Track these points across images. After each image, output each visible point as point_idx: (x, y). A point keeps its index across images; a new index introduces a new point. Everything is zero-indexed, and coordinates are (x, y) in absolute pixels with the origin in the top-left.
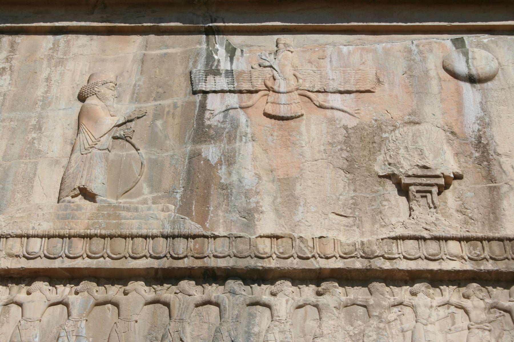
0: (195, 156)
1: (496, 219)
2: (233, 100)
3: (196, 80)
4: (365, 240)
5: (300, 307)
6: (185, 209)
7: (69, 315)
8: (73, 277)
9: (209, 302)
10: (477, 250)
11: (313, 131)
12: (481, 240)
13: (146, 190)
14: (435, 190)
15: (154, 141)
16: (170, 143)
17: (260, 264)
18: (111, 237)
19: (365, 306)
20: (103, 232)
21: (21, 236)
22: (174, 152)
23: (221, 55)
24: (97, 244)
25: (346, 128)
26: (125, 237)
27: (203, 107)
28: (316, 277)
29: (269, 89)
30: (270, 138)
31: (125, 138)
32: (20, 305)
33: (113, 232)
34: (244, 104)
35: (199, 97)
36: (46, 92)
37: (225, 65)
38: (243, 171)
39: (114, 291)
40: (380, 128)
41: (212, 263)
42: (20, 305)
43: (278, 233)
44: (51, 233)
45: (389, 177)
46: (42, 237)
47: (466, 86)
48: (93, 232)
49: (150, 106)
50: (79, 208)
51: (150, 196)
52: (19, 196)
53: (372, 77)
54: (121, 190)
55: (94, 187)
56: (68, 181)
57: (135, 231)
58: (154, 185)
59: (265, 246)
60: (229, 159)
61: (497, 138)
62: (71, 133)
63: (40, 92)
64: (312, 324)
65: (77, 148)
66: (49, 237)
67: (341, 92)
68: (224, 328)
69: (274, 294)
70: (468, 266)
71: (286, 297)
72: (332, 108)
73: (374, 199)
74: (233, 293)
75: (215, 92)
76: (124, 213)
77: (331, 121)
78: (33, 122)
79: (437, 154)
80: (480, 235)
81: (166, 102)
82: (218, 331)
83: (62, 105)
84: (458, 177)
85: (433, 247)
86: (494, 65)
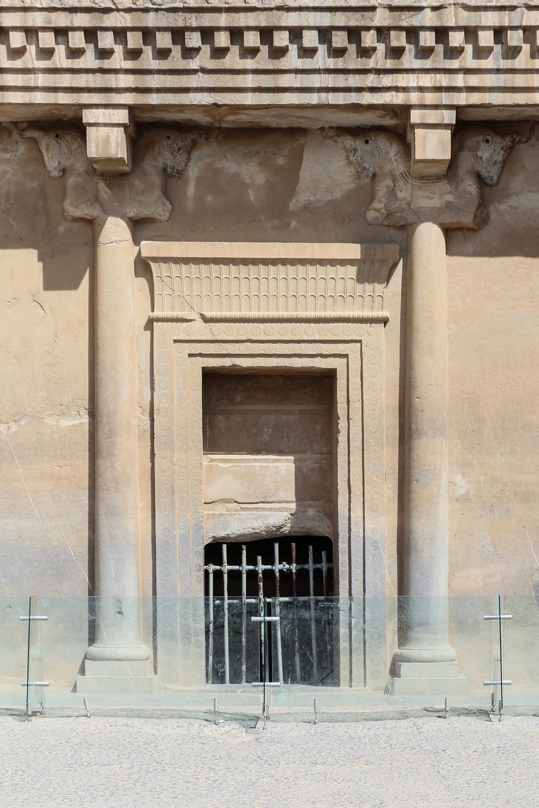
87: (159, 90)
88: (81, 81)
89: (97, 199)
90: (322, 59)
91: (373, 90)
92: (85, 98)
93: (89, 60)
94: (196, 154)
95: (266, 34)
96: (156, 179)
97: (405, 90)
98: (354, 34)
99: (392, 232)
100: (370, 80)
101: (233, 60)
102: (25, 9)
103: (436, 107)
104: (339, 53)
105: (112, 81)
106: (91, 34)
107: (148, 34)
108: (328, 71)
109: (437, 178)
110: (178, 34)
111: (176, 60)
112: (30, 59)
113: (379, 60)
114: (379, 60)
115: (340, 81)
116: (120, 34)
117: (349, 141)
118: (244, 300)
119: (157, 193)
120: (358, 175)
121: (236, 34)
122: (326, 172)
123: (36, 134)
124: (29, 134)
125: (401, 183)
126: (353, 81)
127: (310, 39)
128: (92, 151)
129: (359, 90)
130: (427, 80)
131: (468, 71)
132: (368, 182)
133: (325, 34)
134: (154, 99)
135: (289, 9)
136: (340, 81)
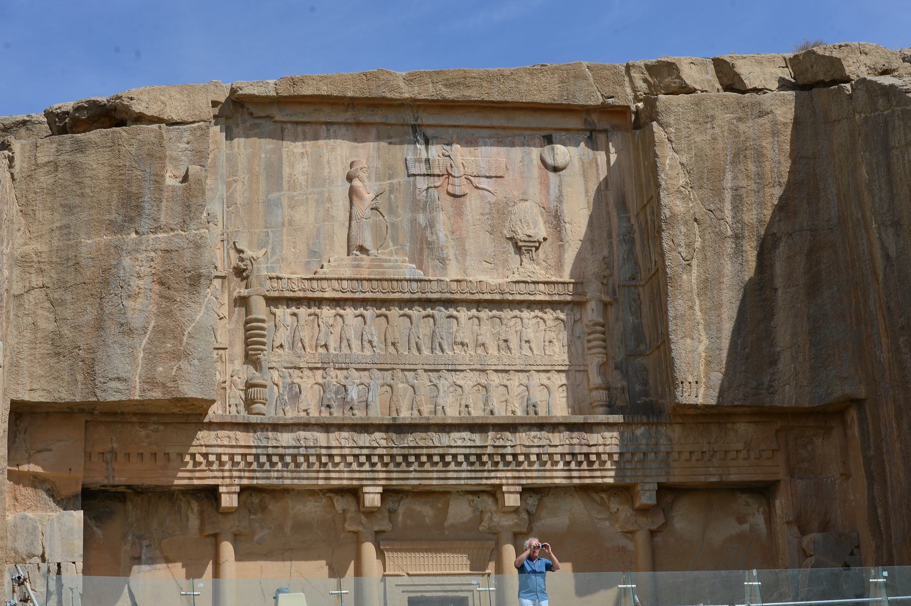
0: (413, 221)
1: (562, 265)
3: (410, 165)
4: (500, 281)
5: (470, 319)
7: (365, 323)
9: (428, 316)
11: (473, 204)
12: (553, 283)
13: (391, 244)
14: (534, 249)
17: (452, 296)
18: (381, 280)
19: (500, 318)
20: (377, 277)
21: (337, 279)
22: (403, 218)
24: (375, 284)
25: (489, 203)
26: (387, 280)
27: (415, 185)
28: (479, 304)
29: (449, 174)
30: (451, 209)
31: (376, 209)
32: (341, 316)
33: (381, 277)
34: (436, 184)
35: (412, 179)
36: (329, 173)
38: (438, 232)
40: (507, 203)
41: (430, 296)
42: (341, 316)
43: (459, 278)
44: (353, 276)
45: (511, 239)
46: (348, 280)
47: (551, 175)
48: (372, 277)
50: (362, 260)
51: (393, 248)
52: (328, 247)
53: (503, 166)
54: (379, 244)
55: (368, 245)
56: (353, 240)
57: (392, 277)
58: (395, 241)
60: (431, 225)
61: (565, 211)
62: (347, 203)
63: (326, 171)
64: (476, 327)
65: (354, 217)
66: (352, 280)
67: (487, 177)
68: (437, 330)
69: (458, 311)
70: (547, 298)
71: (463, 314)
72: (483, 189)
73: (504, 253)
74: (440, 311)
75: (420, 175)
76: (385, 264)
77: (482, 197)
78: (326, 195)
80: (553, 279)
81: (394, 181)
82: (434, 332)
83: (340, 184)
84: (545, 239)
85: (532, 286)
86: (568, 158)
87: (396, 479)
88: (363, 475)
89: (361, 523)
90: (464, 466)
91: (487, 478)
92: (365, 482)
93: (367, 467)
94: (402, 503)
95: (442, 456)
96: (387, 514)
97: (500, 478)
98: (479, 456)
99: (490, 535)
100: (486, 474)
101: (427, 467)
102: (341, 447)
103: (513, 485)
104: (472, 464)
105: (376, 475)
106: (368, 457)
107: (392, 456)
108: (468, 471)
109: (511, 512)
110: (405, 457)
111: (403, 467)
112: (342, 467)
113: (489, 466)
114: (489, 466)
115: (473, 475)
116: (381, 456)
117: (470, 497)
118: (426, 567)
119: (387, 520)
120: (474, 511)
121: (430, 456)
122: (460, 511)
123: (332, 495)
124: (328, 495)
125: (495, 515)
126: (479, 475)
127: (461, 458)
128: (368, 503)
129: (481, 478)
130: (509, 474)
131: (526, 471)
132: (480, 515)
133: (467, 456)
134: (394, 482)
135: (451, 447)
136: (473, 475)
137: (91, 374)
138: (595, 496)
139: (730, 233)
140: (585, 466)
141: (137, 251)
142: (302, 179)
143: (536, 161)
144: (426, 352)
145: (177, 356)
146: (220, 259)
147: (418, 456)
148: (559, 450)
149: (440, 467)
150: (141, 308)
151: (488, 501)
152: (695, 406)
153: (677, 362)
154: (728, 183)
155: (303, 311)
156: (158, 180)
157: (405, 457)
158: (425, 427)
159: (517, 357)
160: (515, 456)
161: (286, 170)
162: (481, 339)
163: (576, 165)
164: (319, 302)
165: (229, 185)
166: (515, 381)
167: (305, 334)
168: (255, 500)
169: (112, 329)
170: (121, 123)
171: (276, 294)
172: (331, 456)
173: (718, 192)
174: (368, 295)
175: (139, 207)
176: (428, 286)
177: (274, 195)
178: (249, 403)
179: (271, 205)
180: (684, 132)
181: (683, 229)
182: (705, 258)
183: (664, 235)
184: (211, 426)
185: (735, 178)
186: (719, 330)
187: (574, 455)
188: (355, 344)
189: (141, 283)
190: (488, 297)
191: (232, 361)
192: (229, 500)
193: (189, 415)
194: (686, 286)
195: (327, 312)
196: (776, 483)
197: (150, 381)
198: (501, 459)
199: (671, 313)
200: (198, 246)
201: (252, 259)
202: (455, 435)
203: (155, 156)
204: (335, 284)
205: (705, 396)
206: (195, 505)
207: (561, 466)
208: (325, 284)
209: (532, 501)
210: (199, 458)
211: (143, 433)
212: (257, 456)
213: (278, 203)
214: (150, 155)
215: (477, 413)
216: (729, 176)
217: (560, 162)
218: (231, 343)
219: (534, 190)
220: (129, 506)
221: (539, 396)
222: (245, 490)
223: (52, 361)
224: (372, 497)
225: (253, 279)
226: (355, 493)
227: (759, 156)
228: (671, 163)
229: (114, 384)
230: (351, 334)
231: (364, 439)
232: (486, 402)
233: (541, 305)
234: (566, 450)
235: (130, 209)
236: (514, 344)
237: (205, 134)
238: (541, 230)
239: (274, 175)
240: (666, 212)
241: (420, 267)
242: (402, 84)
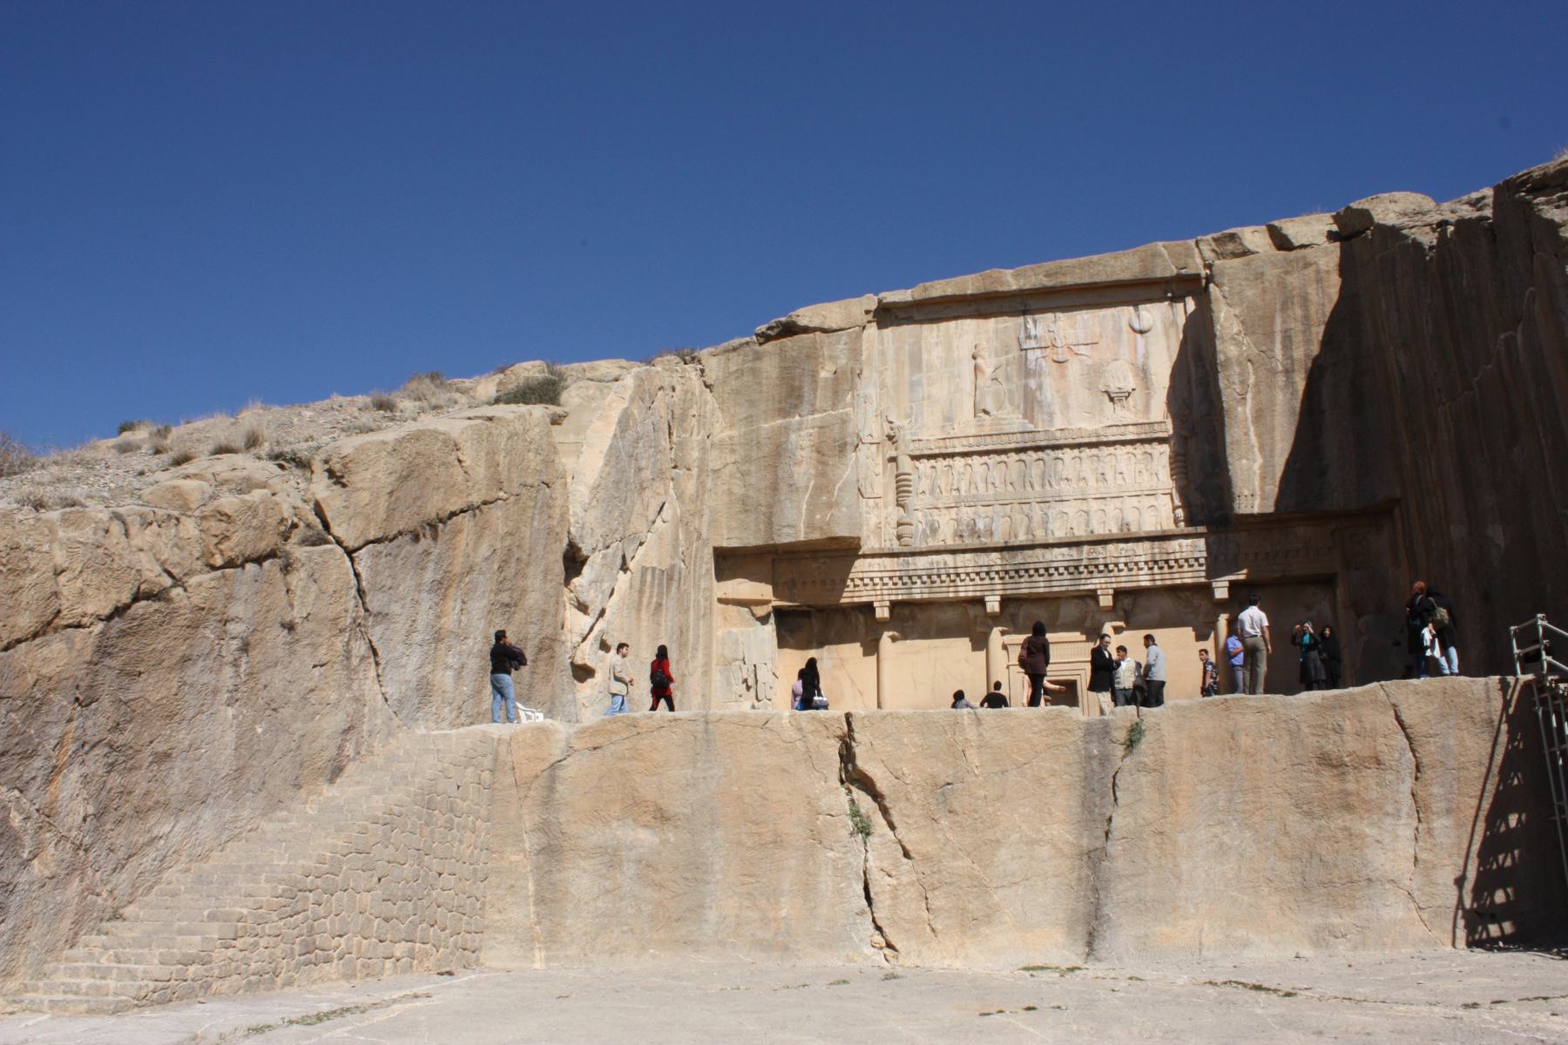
0: (1026, 386)
2: (1038, 353)
6: (1025, 416)
8: (987, 453)
10: (1140, 429)
15: (1008, 378)
16: (1015, 379)
22: (1017, 382)
23: (1030, 325)
28: (1079, 446)
37: (1033, 333)
39: (1003, 457)
49: (1003, 359)
58: (1011, 402)
59: (1058, 434)
60: (1040, 387)
71: (1068, 454)
79: (1125, 378)
90: (1066, 576)
93: (987, 581)
95: (1047, 569)
98: (1076, 568)
107: (1007, 572)
110: (1017, 571)
121: (1037, 570)
122: (1069, 611)
133: (1066, 568)
137: (770, 523)
138: (1182, 595)
139: (1280, 368)
140: (1166, 570)
141: (799, 429)
142: (937, 362)
143: (1126, 328)
144: (1037, 488)
145: (830, 505)
146: (873, 429)
147: (1027, 571)
148: (1143, 558)
149: (1046, 578)
150: (803, 470)
151: (1091, 603)
152: (1252, 515)
153: (1234, 480)
154: (1278, 327)
155: (941, 463)
156: (814, 376)
157: (1017, 571)
158: (1032, 547)
159: (1112, 487)
160: (1106, 566)
161: (925, 357)
162: (1082, 475)
163: (1159, 328)
164: (952, 455)
165: (881, 373)
166: (1111, 507)
167: (942, 482)
168: (906, 611)
169: (783, 487)
170: (796, 333)
171: (918, 453)
172: (958, 575)
173: (1270, 335)
174: (990, 447)
175: (800, 397)
176: (1038, 436)
177: (915, 378)
178: (899, 537)
179: (914, 385)
180: (1238, 289)
181: (1237, 369)
182: (1259, 392)
183: (1221, 376)
184: (865, 556)
185: (1284, 322)
186: (1272, 450)
187: (1156, 562)
188: (981, 486)
189: (803, 453)
190: (1086, 440)
191: (886, 507)
192: (882, 613)
193: (844, 551)
194: (1241, 416)
195: (959, 462)
196: (1335, 574)
197: (810, 526)
198: (1093, 568)
199: (1228, 440)
200: (844, 422)
201: (899, 428)
202: (1056, 551)
203: (812, 356)
204: (964, 441)
205: (1260, 506)
206: (861, 618)
207: (1146, 571)
208: (956, 442)
209: (1127, 602)
210: (858, 582)
211: (815, 565)
212: (901, 578)
213: (919, 383)
214: (808, 357)
215: (1081, 533)
216: (1278, 321)
217: (1145, 326)
218: (886, 493)
219: (1125, 352)
220: (814, 620)
221: (1131, 517)
222: (894, 605)
223: (742, 516)
224: (993, 605)
225: (900, 443)
226: (981, 602)
227: (1305, 300)
228: (1227, 319)
229: (786, 530)
230: (978, 479)
231: (984, 559)
232: (1087, 525)
233: (1132, 442)
234: (1148, 558)
235: (791, 397)
236: (1109, 477)
237: (859, 336)
238: (1130, 382)
239: (916, 362)
240: (1221, 357)
241: (1031, 422)
242: (1010, 279)
